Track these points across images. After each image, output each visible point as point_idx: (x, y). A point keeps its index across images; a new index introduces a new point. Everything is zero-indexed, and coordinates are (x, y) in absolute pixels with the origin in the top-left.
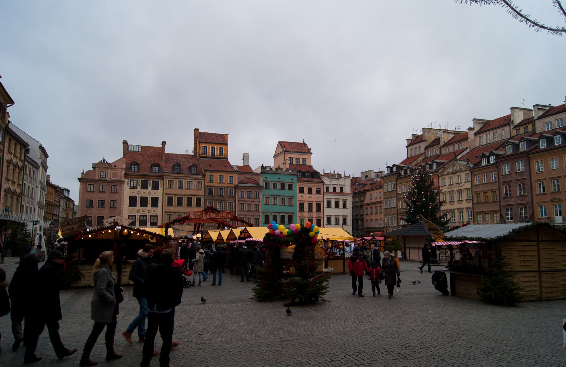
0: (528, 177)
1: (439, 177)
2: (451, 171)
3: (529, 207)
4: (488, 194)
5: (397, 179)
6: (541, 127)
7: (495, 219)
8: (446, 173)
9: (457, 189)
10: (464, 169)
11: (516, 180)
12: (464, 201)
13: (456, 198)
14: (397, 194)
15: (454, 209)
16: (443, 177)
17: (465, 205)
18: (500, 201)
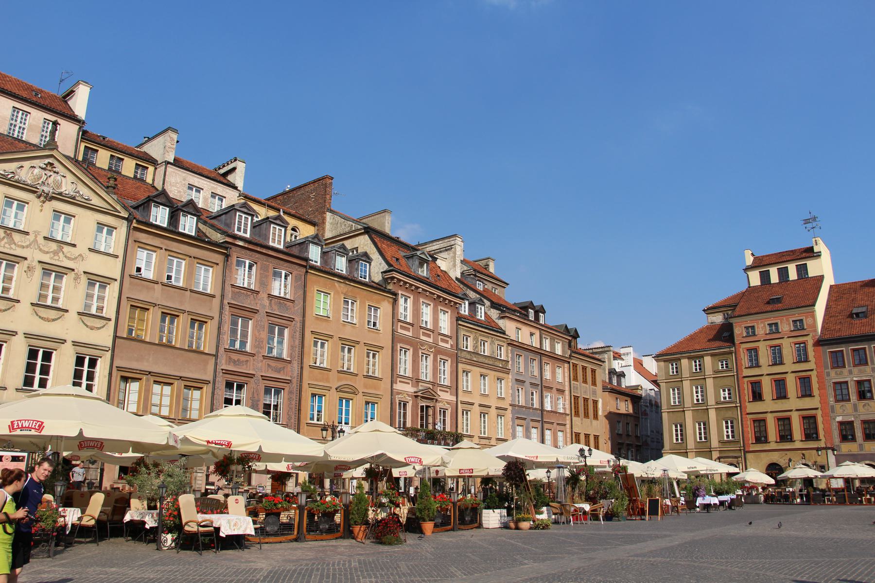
0: (298, 319)
3: (290, 392)
9: (46, 258)
10: (96, 201)
12: (72, 316)
15: (14, 333)
17: (70, 328)
18: (216, 356)
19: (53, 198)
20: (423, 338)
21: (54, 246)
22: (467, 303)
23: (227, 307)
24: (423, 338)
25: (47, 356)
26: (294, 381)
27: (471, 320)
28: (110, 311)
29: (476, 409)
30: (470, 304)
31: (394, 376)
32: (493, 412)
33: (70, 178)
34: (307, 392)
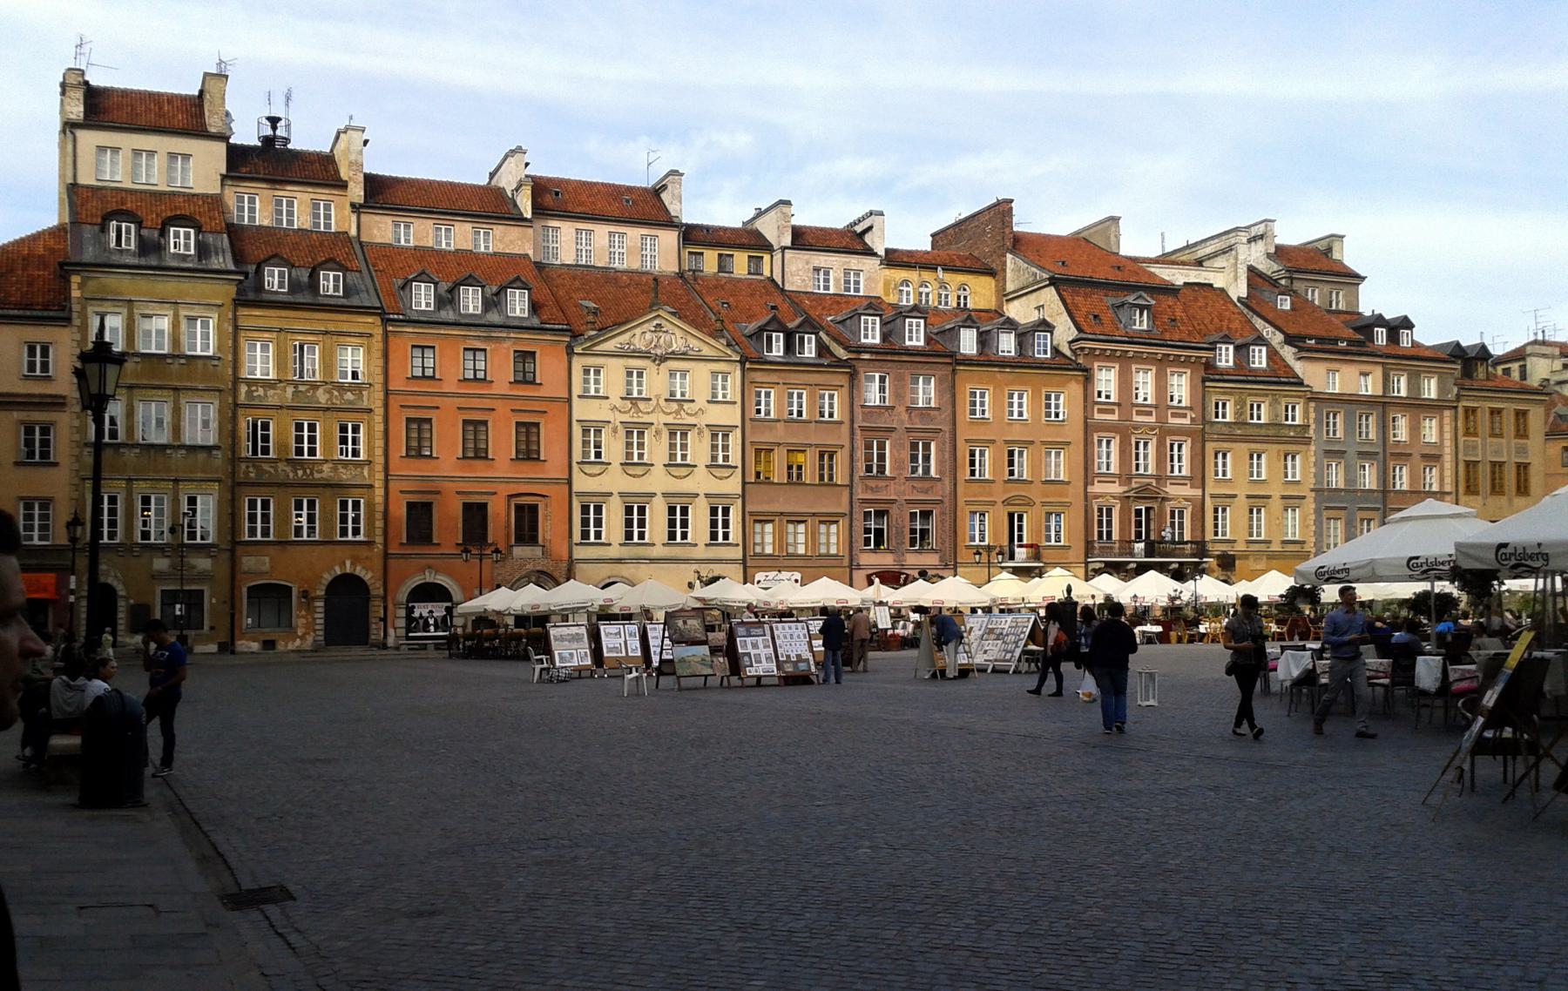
0: (946, 428)
1: (570, 352)
2: (639, 344)
3: (943, 513)
4: (800, 458)
5: (241, 302)
6: (798, 272)
7: (823, 539)
8: (610, 346)
9: (670, 419)
10: (707, 351)
11: (908, 430)
12: (701, 471)
13: (656, 449)
14: (236, 380)
15: (653, 495)
16: (591, 361)
17: (701, 482)
18: (851, 486)
19: (667, 359)
20: (1137, 418)
21: (675, 406)
22: (1231, 348)
23: (858, 432)
24: (1137, 418)
25: (685, 511)
26: (946, 500)
27: (1242, 375)
28: (735, 458)
29: (1242, 503)
30: (1237, 348)
31: (1089, 476)
32: (1276, 504)
33: (677, 331)
34: (964, 511)
